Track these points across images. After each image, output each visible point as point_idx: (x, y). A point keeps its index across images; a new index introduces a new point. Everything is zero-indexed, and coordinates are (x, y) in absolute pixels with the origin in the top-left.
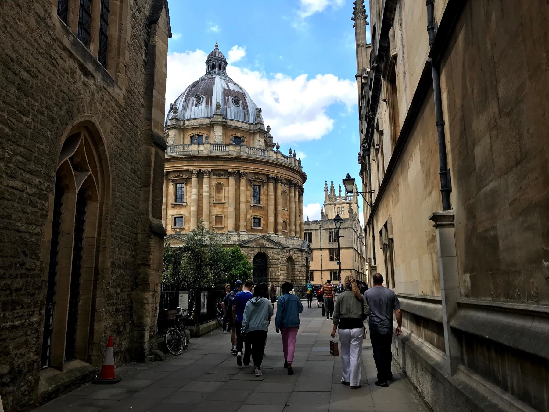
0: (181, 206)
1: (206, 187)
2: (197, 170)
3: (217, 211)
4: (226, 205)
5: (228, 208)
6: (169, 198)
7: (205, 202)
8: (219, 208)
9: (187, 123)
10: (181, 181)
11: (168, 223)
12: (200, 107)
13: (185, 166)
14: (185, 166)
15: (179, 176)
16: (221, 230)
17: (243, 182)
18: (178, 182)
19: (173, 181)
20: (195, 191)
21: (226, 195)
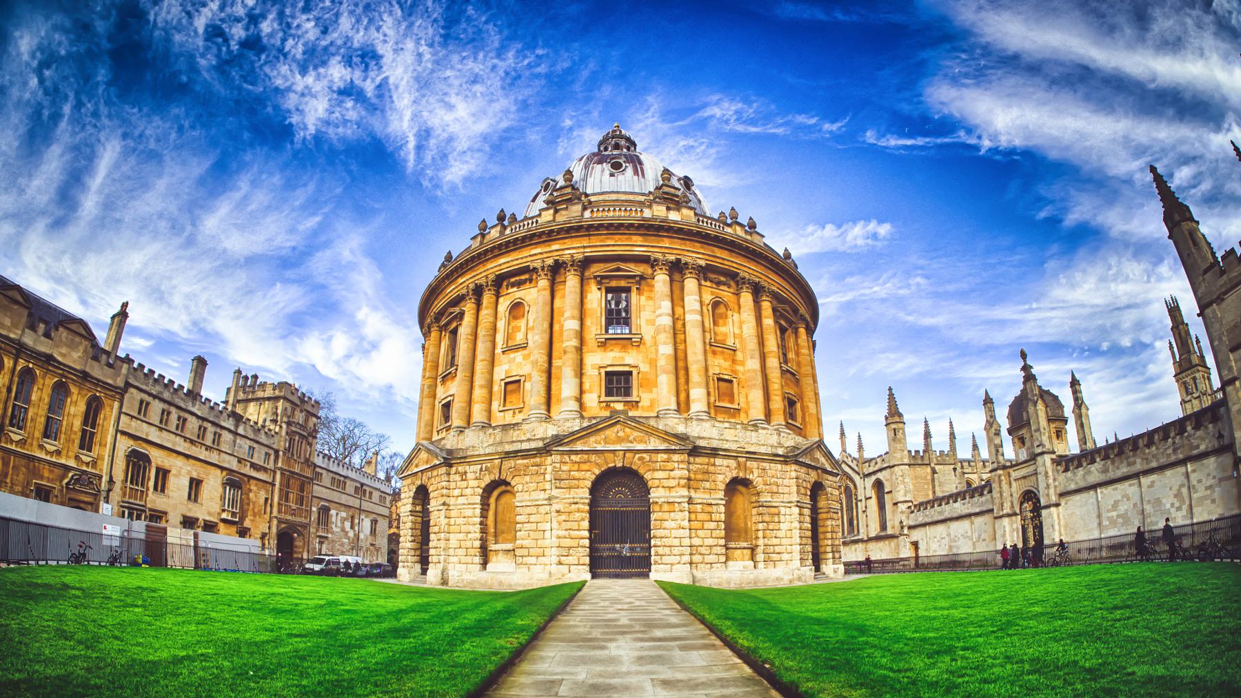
0: (627, 342)
1: (691, 301)
2: (672, 258)
3: (719, 365)
4: (739, 356)
5: (743, 363)
6: (588, 322)
7: (694, 336)
8: (725, 360)
9: (593, 199)
10: (623, 283)
11: (586, 386)
12: (621, 177)
13: (637, 245)
14: (637, 245)
15: (618, 269)
16: (734, 416)
17: (766, 306)
18: (614, 284)
19: (600, 280)
20: (666, 305)
21: (737, 331)
